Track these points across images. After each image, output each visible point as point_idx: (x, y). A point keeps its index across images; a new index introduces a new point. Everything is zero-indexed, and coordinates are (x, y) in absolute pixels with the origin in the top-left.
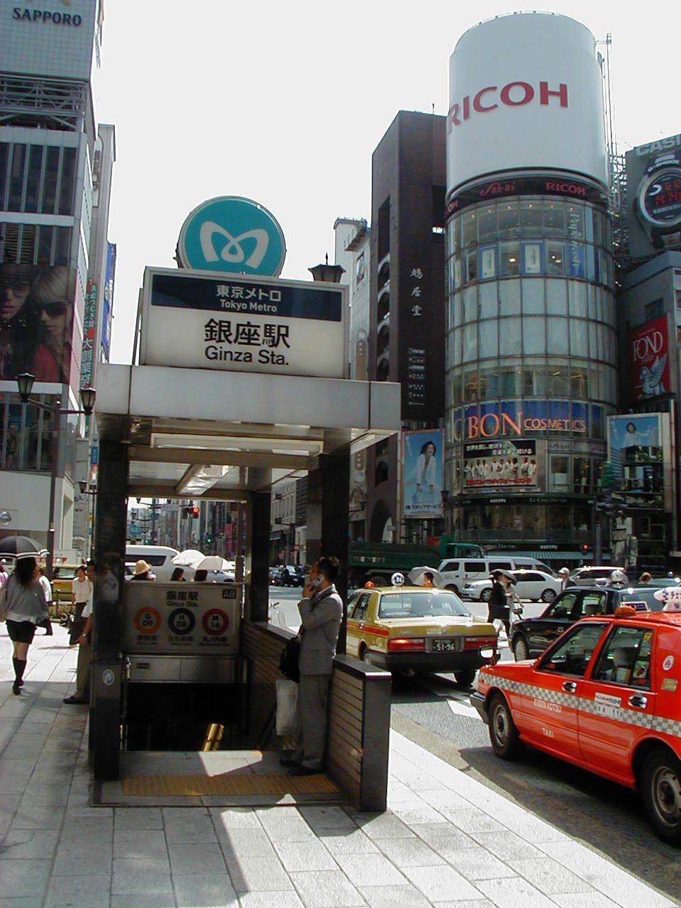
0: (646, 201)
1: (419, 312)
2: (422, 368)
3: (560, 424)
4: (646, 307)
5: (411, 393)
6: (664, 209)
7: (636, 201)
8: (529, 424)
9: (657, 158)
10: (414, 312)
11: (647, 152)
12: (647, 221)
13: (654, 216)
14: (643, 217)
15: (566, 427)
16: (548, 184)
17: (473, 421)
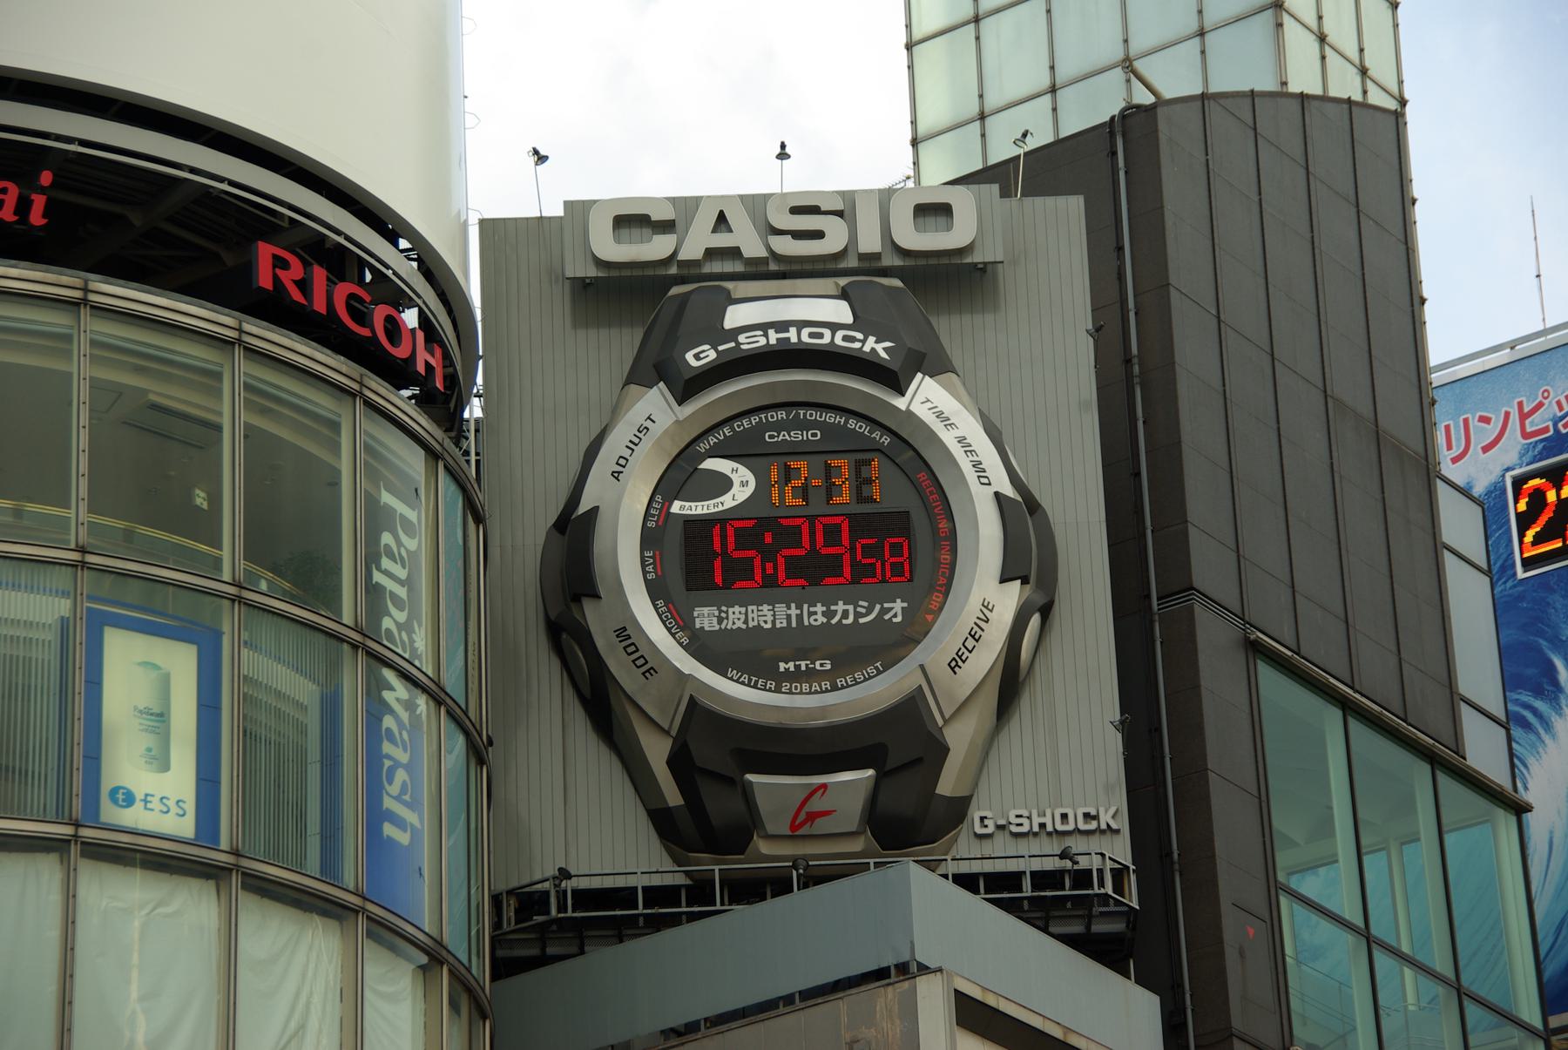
0: (649, 539)
6: (765, 616)
11: (657, 248)
12: (647, 662)
13: (699, 646)
14: (627, 634)
16: (265, 252)
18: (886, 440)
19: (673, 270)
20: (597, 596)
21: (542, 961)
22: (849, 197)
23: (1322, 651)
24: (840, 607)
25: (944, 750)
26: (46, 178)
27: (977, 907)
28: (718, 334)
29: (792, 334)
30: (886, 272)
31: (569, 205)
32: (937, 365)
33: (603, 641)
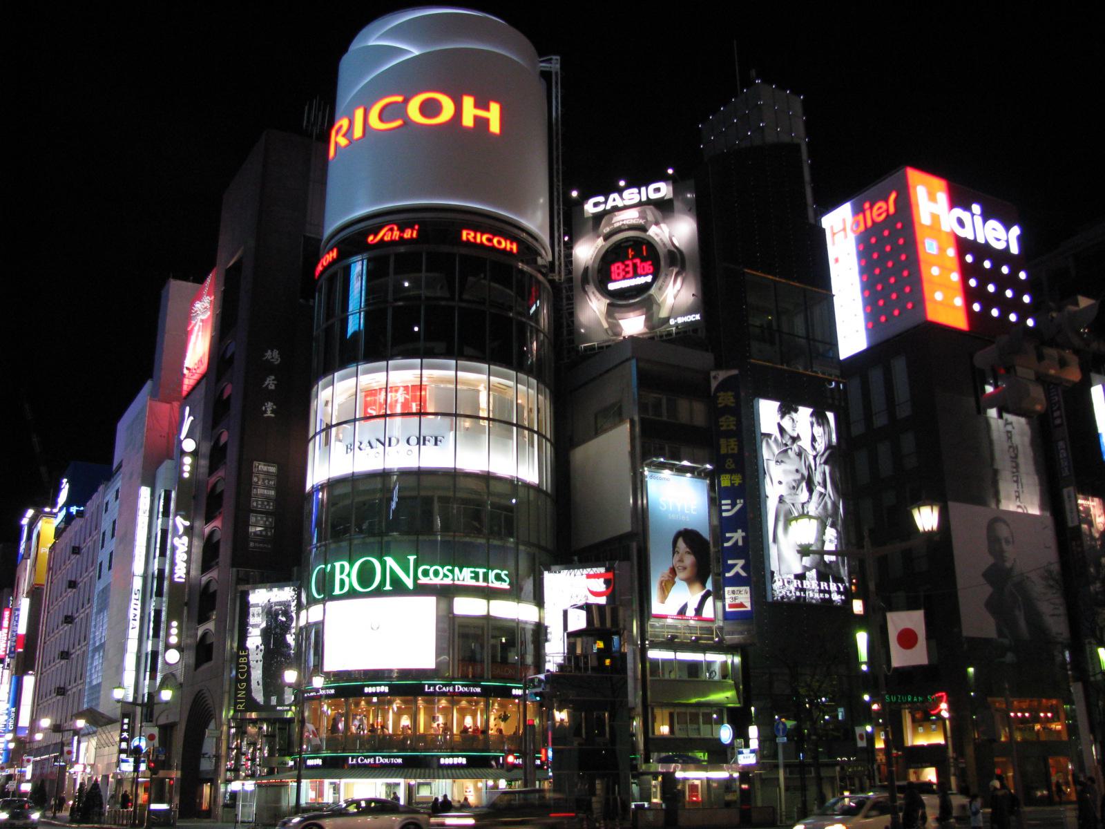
1: (273, 411)
2: (272, 493)
3: (473, 575)
8: (426, 573)
10: (265, 412)
17: (342, 567)
26: (417, 227)
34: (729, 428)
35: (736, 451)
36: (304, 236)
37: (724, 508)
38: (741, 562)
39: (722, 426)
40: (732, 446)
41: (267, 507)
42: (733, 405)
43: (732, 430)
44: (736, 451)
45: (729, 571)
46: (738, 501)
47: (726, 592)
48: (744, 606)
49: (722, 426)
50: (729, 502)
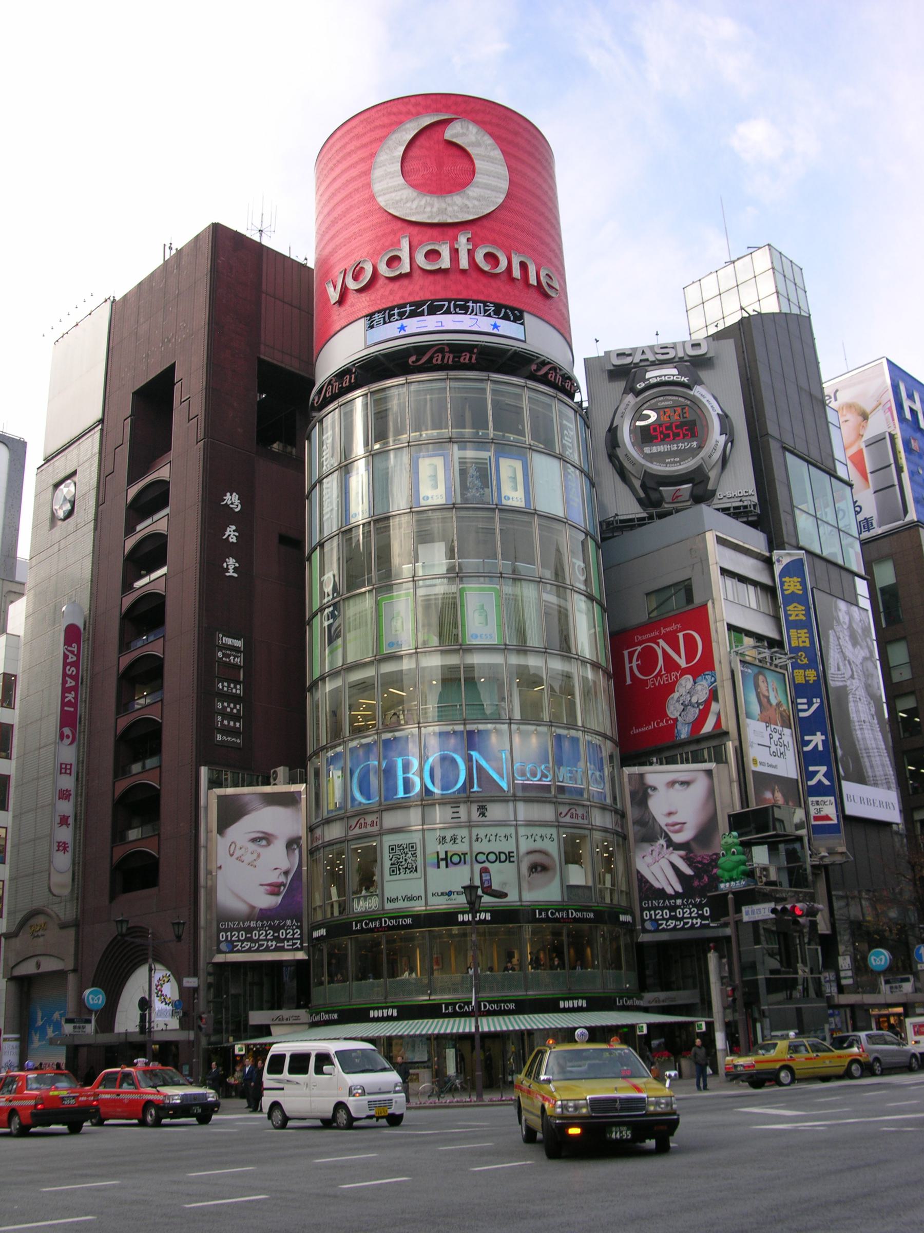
1: (235, 570)
3: (569, 775)
4: (648, 594)
5: (220, 718)
6: (662, 448)
7: (613, 432)
9: (647, 371)
10: (227, 570)
11: (628, 360)
12: (634, 463)
15: (579, 782)
18: (689, 402)
19: (632, 365)
20: (619, 447)
21: (613, 537)
22: (675, 344)
23: (801, 448)
24: (680, 445)
25: (709, 478)
27: (721, 515)
28: (644, 380)
29: (663, 378)
30: (686, 361)
31: (605, 352)
32: (699, 382)
33: (622, 458)
34: (797, 618)
35: (807, 644)
36: (259, 358)
37: (800, 707)
38: (823, 769)
39: (791, 615)
40: (804, 639)
41: (234, 691)
42: (801, 592)
43: (801, 620)
44: (807, 644)
45: (811, 779)
46: (814, 700)
47: (810, 803)
48: (830, 819)
49: (791, 615)
50: (805, 700)
